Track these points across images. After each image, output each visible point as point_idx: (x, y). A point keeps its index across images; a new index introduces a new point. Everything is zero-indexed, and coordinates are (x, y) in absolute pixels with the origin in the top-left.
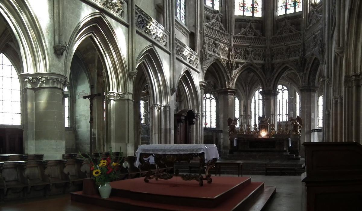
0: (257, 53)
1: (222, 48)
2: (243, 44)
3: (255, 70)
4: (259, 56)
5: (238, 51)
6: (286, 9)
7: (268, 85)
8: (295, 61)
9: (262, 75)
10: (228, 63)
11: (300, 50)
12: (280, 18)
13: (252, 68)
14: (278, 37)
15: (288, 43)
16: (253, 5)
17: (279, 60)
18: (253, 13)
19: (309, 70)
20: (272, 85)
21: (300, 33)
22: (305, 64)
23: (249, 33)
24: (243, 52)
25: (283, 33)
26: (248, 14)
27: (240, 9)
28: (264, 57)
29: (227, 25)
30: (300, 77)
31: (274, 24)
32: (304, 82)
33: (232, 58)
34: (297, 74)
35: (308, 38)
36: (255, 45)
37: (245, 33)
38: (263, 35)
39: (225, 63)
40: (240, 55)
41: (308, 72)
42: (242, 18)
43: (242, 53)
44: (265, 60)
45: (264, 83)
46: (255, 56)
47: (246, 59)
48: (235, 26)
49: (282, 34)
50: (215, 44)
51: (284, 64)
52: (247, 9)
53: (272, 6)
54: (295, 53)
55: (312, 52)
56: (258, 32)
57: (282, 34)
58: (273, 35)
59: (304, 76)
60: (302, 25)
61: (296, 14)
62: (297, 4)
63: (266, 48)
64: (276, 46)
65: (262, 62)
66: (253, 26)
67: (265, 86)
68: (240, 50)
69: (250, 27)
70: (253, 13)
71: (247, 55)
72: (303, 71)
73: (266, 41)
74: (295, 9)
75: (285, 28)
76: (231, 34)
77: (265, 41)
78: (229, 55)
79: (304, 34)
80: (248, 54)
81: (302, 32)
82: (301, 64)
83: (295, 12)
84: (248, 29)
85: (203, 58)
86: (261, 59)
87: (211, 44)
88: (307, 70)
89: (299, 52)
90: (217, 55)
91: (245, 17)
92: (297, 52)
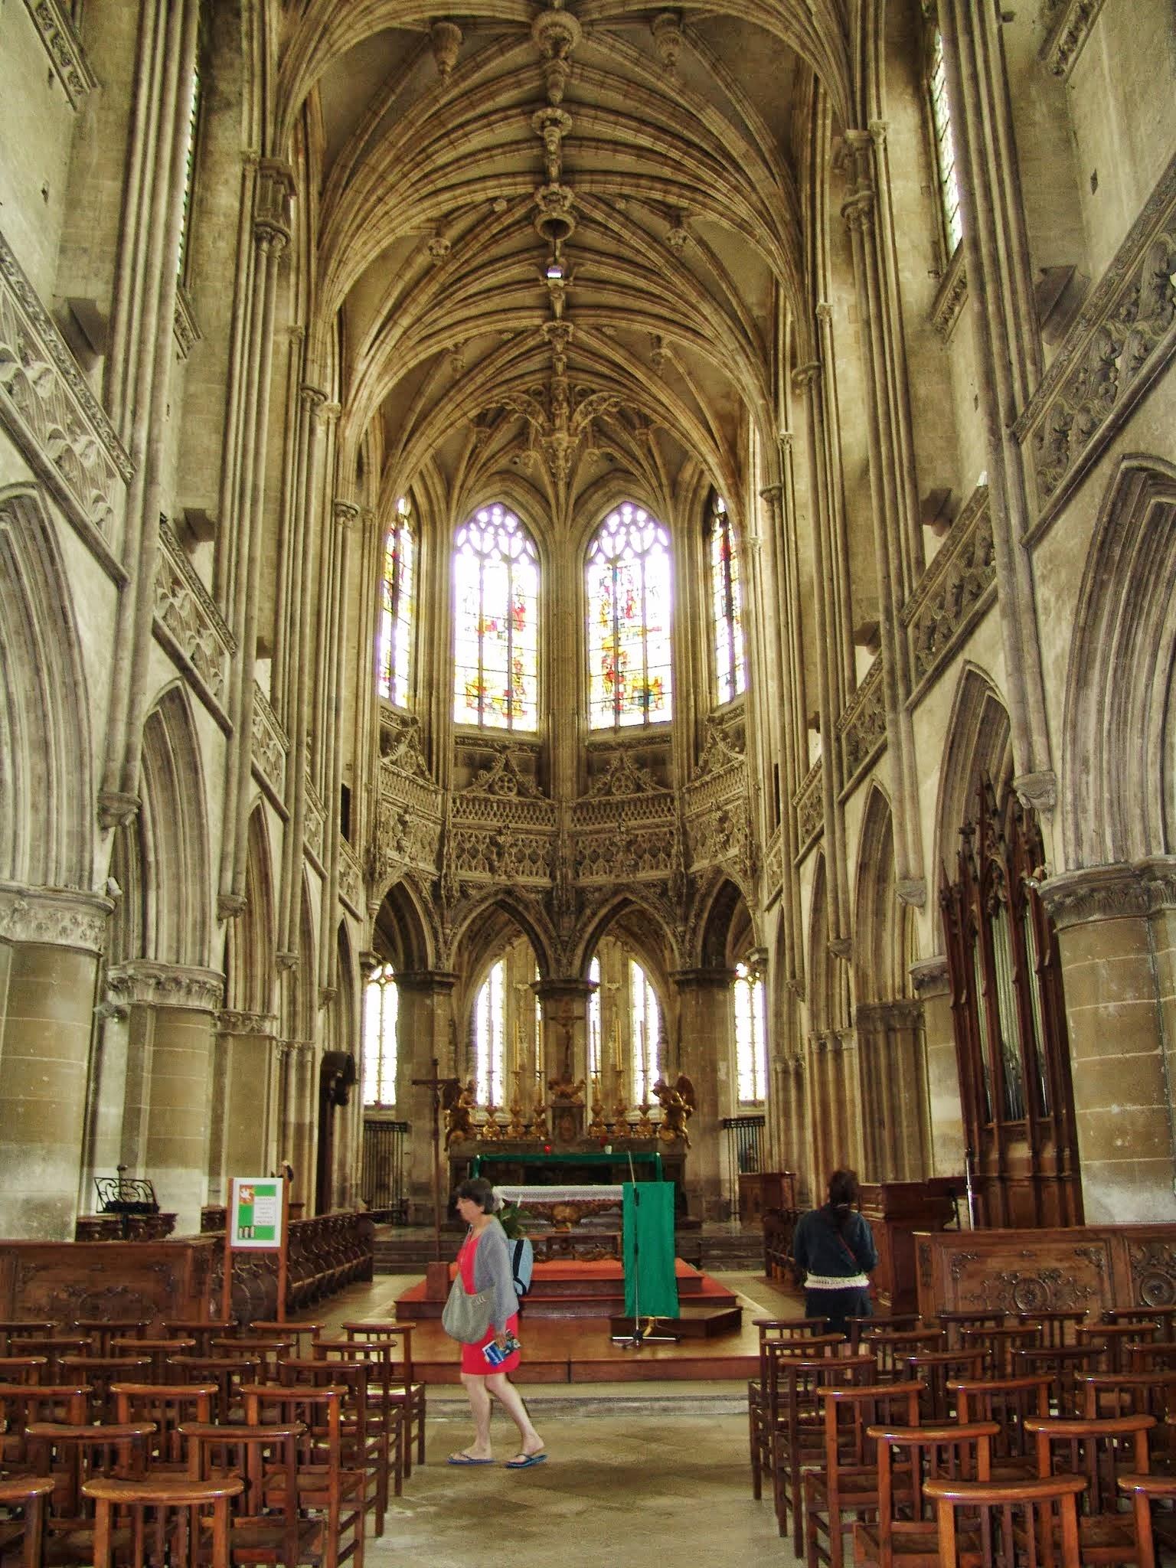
0: (528, 852)
1: (420, 835)
2: (483, 822)
3: (520, 908)
4: (534, 862)
5: (467, 846)
6: (617, 710)
7: (565, 961)
8: (655, 886)
9: (546, 931)
10: (436, 886)
11: (674, 851)
12: (598, 738)
13: (510, 901)
14: (595, 801)
15: (633, 823)
16: (509, 693)
17: (600, 879)
18: (509, 716)
19: (706, 915)
20: (577, 962)
21: (668, 795)
22: (691, 896)
23: (502, 788)
24: (481, 847)
25: (614, 790)
26: (495, 720)
27: (469, 705)
28: (552, 865)
29: (434, 758)
30: (675, 936)
31: (579, 757)
32: (690, 956)
33: (449, 866)
34: (665, 926)
35: (698, 816)
36: (520, 826)
37: (490, 786)
38: (547, 794)
39: (428, 885)
40: (474, 857)
41: (703, 923)
42: (475, 732)
43: (477, 851)
44: (553, 877)
45: (550, 952)
46: (520, 862)
47: (492, 870)
48: (456, 757)
49: (609, 793)
50: (404, 823)
51: (615, 893)
52: (491, 706)
53: (571, 703)
54: (654, 856)
55: (716, 862)
56: (530, 780)
57: (609, 793)
58: (579, 796)
59: (688, 937)
60: (675, 771)
61: (650, 732)
62: (651, 698)
63: (556, 835)
64: (591, 832)
65: (544, 882)
66: (514, 763)
68: (473, 839)
69: (507, 767)
70: (509, 716)
71: (495, 857)
72: (686, 919)
73: (556, 813)
74: (646, 712)
75: (618, 774)
76: (445, 788)
77: (552, 811)
79: (682, 798)
80: (500, 855)
81: (677, 794)
82: (680, 896)
83: (647, 725)
84: (501, 773)
85: (372, 875)
86: (541, 872)
87: (392, 823)
88: (698, 916)
89: (669, 855)
90: (407, 860)
91: (487, 733)
92: (662, 855)
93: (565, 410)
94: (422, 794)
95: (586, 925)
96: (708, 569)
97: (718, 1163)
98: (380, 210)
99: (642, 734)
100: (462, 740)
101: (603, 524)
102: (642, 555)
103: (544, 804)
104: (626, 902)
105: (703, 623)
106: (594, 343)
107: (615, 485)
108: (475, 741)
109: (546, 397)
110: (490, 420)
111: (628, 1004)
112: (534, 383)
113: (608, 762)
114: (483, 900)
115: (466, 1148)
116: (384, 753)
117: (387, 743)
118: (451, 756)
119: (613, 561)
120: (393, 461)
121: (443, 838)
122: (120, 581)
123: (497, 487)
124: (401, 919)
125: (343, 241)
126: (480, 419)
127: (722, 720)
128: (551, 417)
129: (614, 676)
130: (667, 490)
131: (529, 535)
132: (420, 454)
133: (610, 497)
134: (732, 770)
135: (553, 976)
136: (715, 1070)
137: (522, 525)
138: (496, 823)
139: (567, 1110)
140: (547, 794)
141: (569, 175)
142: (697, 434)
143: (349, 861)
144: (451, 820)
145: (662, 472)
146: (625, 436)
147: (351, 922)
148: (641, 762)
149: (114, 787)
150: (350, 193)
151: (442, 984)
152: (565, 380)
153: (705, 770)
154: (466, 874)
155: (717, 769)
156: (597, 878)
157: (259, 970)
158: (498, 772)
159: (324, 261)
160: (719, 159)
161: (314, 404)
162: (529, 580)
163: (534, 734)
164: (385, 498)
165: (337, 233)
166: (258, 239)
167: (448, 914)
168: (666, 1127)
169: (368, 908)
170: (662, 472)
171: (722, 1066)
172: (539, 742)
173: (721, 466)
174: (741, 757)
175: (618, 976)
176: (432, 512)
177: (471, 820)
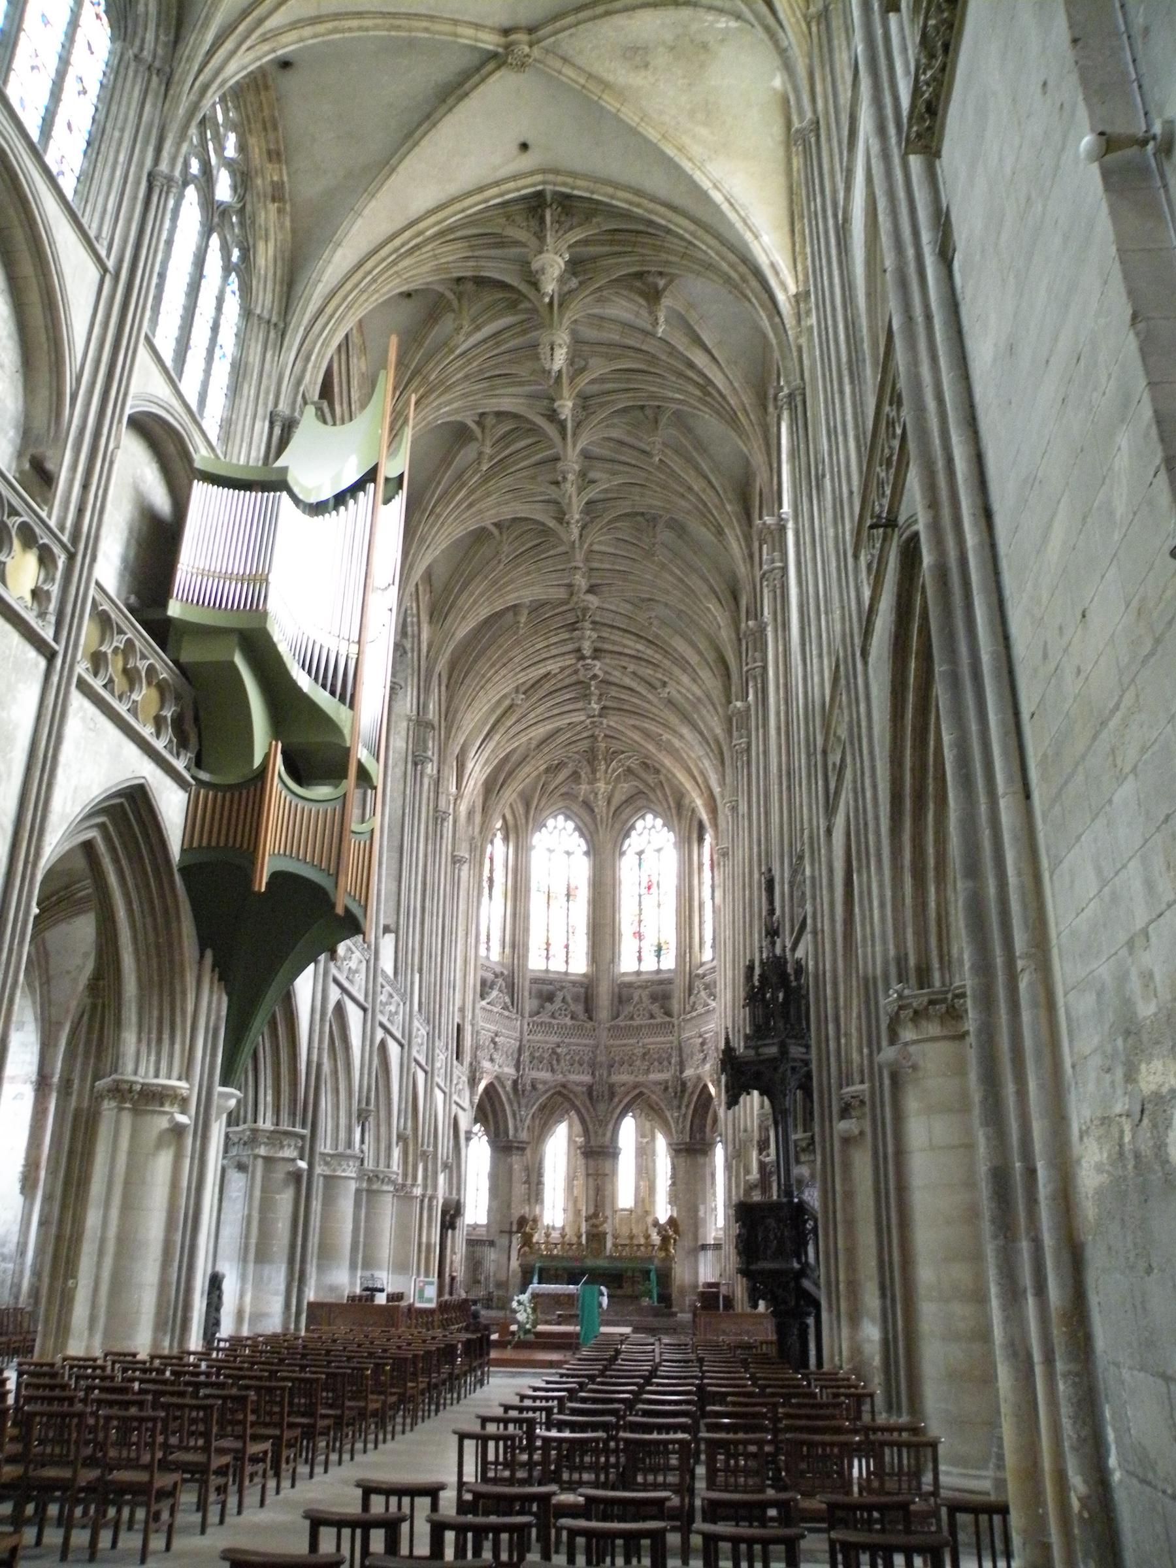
6: (640, 959)
7: (600, 1131)
10: (515, 1082)
12: (627, 979)
14: (622, 1024)
15: (647, 1041)
22: (683, 1091)
24: (546, 1055)
28: (593, 1066)
38: (590, 1018)
41: (690, 1112)
44: (593, 1074)
47: (553, 1071)
49: (632, 1018)
50: (495, 1043)
53: (609, 955)
56: (579, 1008)
57: (632, 1018)
60: (675, 1006)
63: (597, 1047)
65: (587, 1078)
66: (569, 999)
67: (592, 1134)
69: (564, 1000)
72: (679, 1107)
76: (523, 1016)
78: (518, 1061)
80: (558, 1061)
88: (687, 1106)
93: (603, 767)
94: (507, 1022)
95: (615, 1109)
96: (700, 865)
97: (696, 1273)
98: (481, 693)
99: (656, 977)
100: (535, 981)
101: (633, 827)
102: (659, 850)
103: (589, 1025)
104: (641, 1094)
105: (696, 904)
106: (622, 728)
107: (640, 803)
108: (543, 981)
109: (591, 757)
110: (553, 770)
111: (654, 1153)
112: (584, 745)
113: (630, 999)
114: (546, 1091)
115: (531, 1259)
116: (482, 997)
117: (485, 987)
118: (526, 994)
119: (640, 853)
120: (489, 803)
121: (520, 1050)
122: (365, 1010)
123: (560, 804)
124: (492, 1105)
125: (459, 716)
126: (547, 770)
127: (704, 975)
128: (594, 771)
129: (639, 936)
130: (674, 811)
131: (582, 835)
132: (510, 795)
133: (640, 809)
134: (708, 1012)
135: (593, 1143)
136: (696, 1211)
137: (577, 828)
138: (556, 1039)
139: (596, 1237)
140: (590, 1018)
141: (597, 653)
142: (688, 785)
143: (461, 1073)
144: (526, 1037)
145: (670, 799)
146: (644, 775)
147: (461, 1114)
148: (654, 998)
149: (364, 1105)
150: (463, 688)
151: (518, 1148)
152: (603, 745)
153: (693, 1009)
154: (535, 1074)
155: (701, 1010)
156: (622, 1077)
157: (410, 1159)
158: (558, 1003)
159: (449, 730)
160: (683, 664)
161: (443, 820)
162: (580, 870)
163: (584, 975)
164: (485, 826)
165: (456, 712)
166: (415, 764)
167: (523, 1101)
168: (661, 1249)
169: (471, 1102)
170: (670, 799)
171: (702, 1208)
172: (585, 980)
173: (705, 805)
174: (714, 1004)
175: (648, 1132)
176: (516, 826)
177: (539, 1037)
